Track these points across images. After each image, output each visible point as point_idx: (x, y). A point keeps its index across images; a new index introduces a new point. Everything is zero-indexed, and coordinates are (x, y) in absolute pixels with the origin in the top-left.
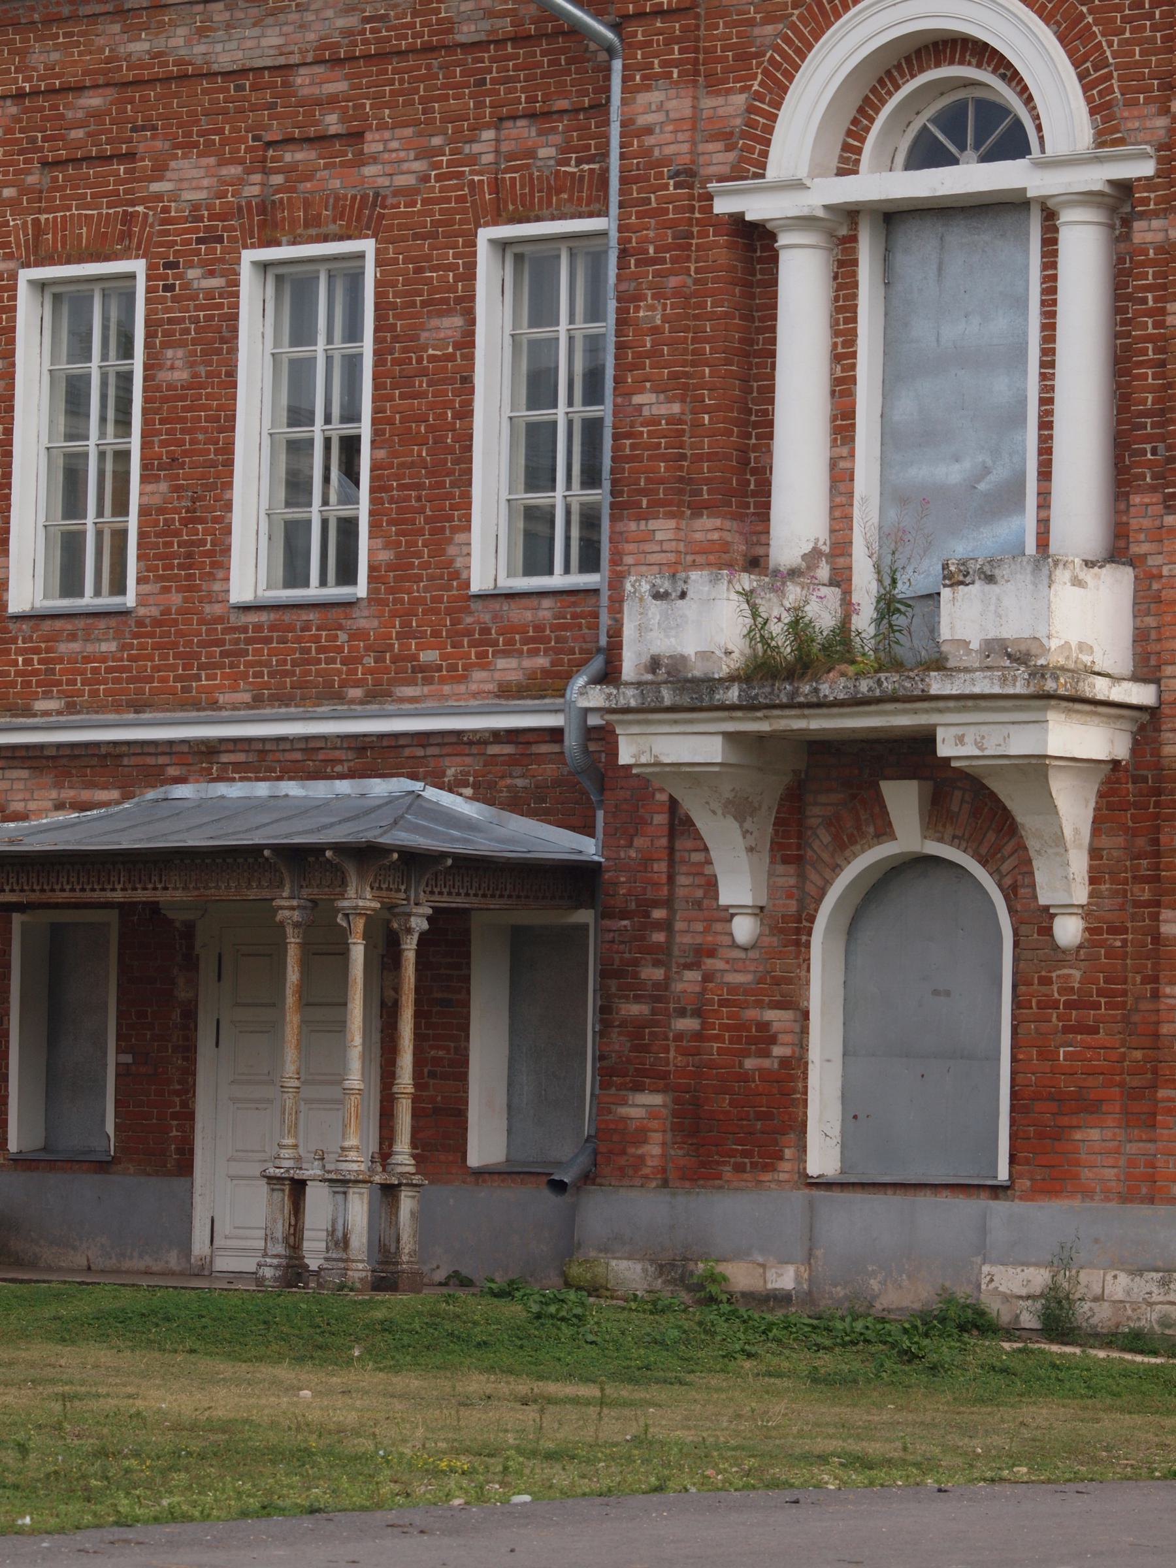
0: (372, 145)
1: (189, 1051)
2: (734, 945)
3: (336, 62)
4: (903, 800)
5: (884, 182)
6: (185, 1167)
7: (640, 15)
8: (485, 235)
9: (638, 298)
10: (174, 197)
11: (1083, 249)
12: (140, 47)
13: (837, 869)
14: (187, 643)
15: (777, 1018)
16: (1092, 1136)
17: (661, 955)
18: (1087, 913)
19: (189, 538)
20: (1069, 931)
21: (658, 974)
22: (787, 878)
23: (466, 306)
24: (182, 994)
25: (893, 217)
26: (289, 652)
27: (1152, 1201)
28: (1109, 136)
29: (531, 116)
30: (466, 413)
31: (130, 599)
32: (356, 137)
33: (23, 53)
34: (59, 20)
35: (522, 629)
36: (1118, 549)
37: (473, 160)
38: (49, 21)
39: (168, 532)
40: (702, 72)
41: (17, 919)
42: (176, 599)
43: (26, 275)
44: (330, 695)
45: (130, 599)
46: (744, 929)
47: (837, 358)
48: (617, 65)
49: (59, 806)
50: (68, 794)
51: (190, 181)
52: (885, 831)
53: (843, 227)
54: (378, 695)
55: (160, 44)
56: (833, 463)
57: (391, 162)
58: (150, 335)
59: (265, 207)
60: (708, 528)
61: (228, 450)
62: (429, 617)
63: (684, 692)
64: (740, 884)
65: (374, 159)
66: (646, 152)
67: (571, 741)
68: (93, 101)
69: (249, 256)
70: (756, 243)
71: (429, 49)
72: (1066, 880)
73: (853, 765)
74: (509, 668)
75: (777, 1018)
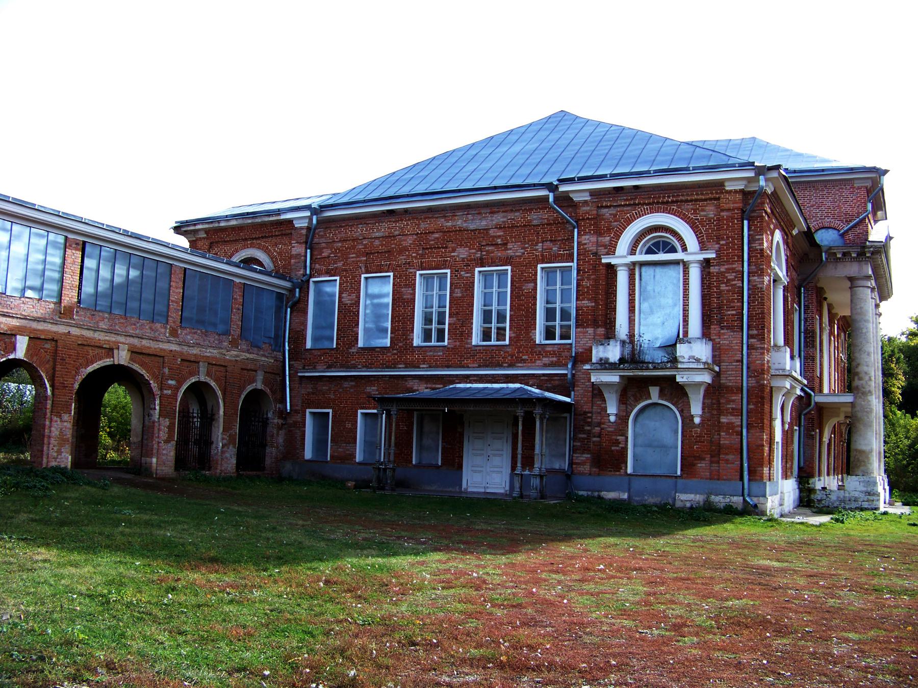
0: (510, 246)
1: (461, 443)
2: (610, 422)
3: (500, 228)
4: (654, 392)
5: (640, 257)
6: (460, 467)
7: (583, 219)
8: (539, 266)
9: (583, 280)
10: (458, 256)
11: (695, 274)
12: (449, 224)
13: (636, 406)
14: (461, 353)
15: (621, 438)
16: (701, 465)
17: (589, 424)
18: (701, 416)
20: (697, 420)
21: (589, 428)
22: (623, 407)
23: (535, 281)
24: (459, 430)
25: (643, 264)
27: (718, 479)
28: (703, 247)
29: (551, 241)
30: (535, 304)
31: (446, 343)
32: (506, 244)
33: (419, 225)
34: (429, 218)
35: (549, 352)
37: (536, 250)
38: (425, 218)
39: (456, 328)
40: (599, 233)
41: (415, 413)
42: (458, 343)
43: (418, 273)
44: (499, 366)
45: (446, 343)
46: (612, 419)
47: (630, 295)
48: (576, 230)
49: (427, 388)
50: (429, 386)
51: (462, 253)
52: (649, 397)
53: (632, 268)
54: (511, 366)
55: (454, 223)
56: (629, 318)
57: (515, 249)
58: (451, 286)
59: (481, 259)
60: (601, 331)
61: (472, 311)
62: (523, 349)
63: (605, 365)
64: (612, 409)
65: (510, 249)
66: (585, 249)
67: (569, 376)
68: (437, 235)
69: (477, 270)
70: (611, 270)
71: (525, 226)
72: (696, 409)
74: (546, 360)
75: (621, 438)
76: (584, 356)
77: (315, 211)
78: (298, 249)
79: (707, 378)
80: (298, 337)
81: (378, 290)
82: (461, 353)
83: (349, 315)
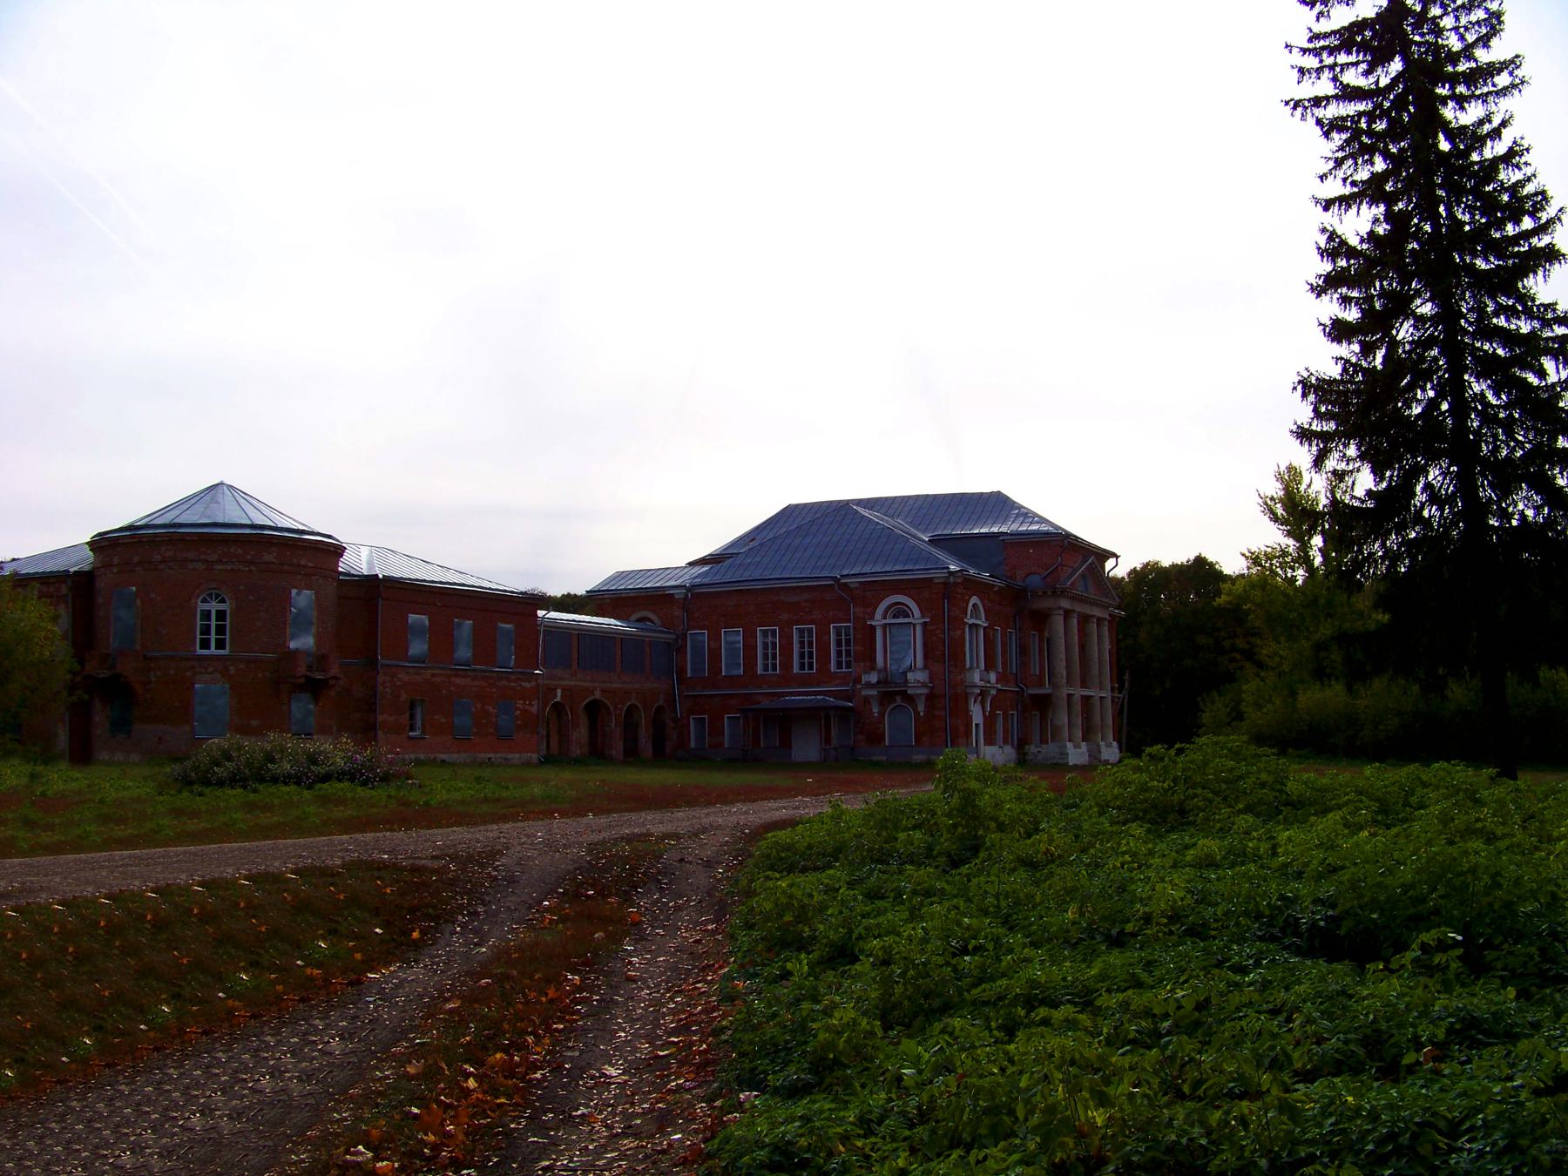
4: (898, 698)
11: (919, 630)
14: (787, 678)
19: (786, 664)
26: (804, 680)
28: (923, 616)
36: (926, 667)
44: (811, 685)
51: (785, 617)
53: (884, 627)
54: (818, 685)
62: (824, 675)
63: (869, 685)
64: (875, 710)
70: (873, 628)
72: (921, 708)
73: (893, 692)
76: (858, 680)
77: (689, 589)
78: (678, 612)
79: (925, 691)
80: (682, 671)
81: (733, 637)
82: (787, 678)
83: (715, 656)
